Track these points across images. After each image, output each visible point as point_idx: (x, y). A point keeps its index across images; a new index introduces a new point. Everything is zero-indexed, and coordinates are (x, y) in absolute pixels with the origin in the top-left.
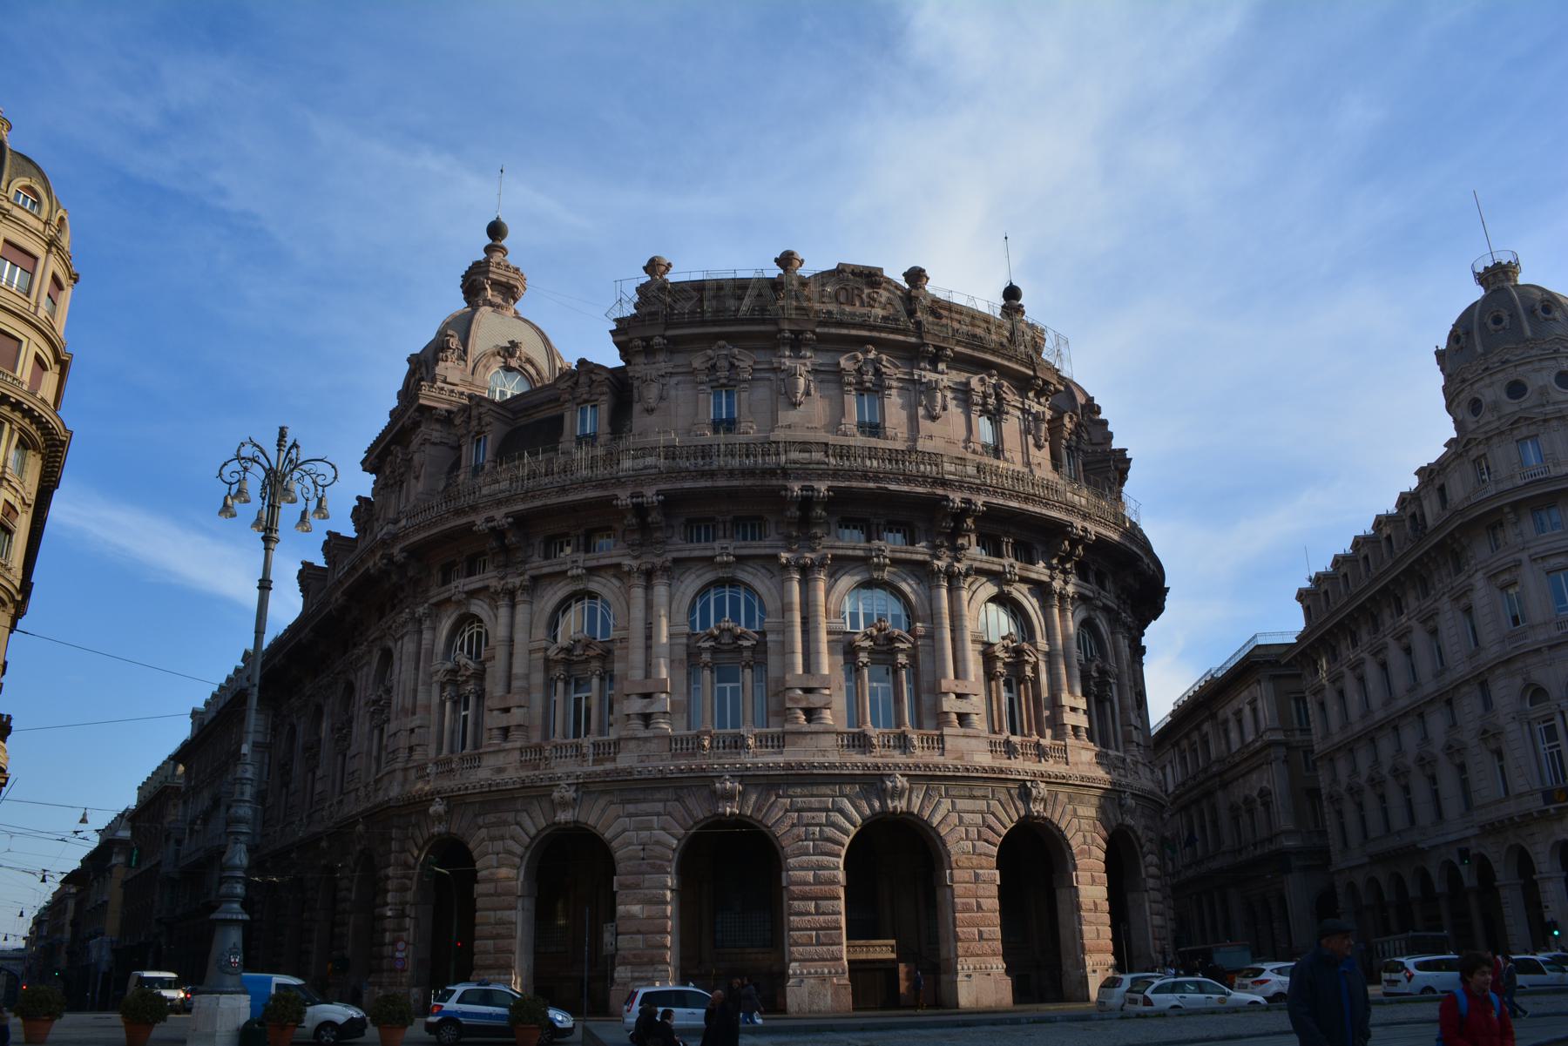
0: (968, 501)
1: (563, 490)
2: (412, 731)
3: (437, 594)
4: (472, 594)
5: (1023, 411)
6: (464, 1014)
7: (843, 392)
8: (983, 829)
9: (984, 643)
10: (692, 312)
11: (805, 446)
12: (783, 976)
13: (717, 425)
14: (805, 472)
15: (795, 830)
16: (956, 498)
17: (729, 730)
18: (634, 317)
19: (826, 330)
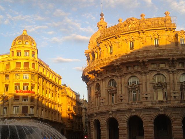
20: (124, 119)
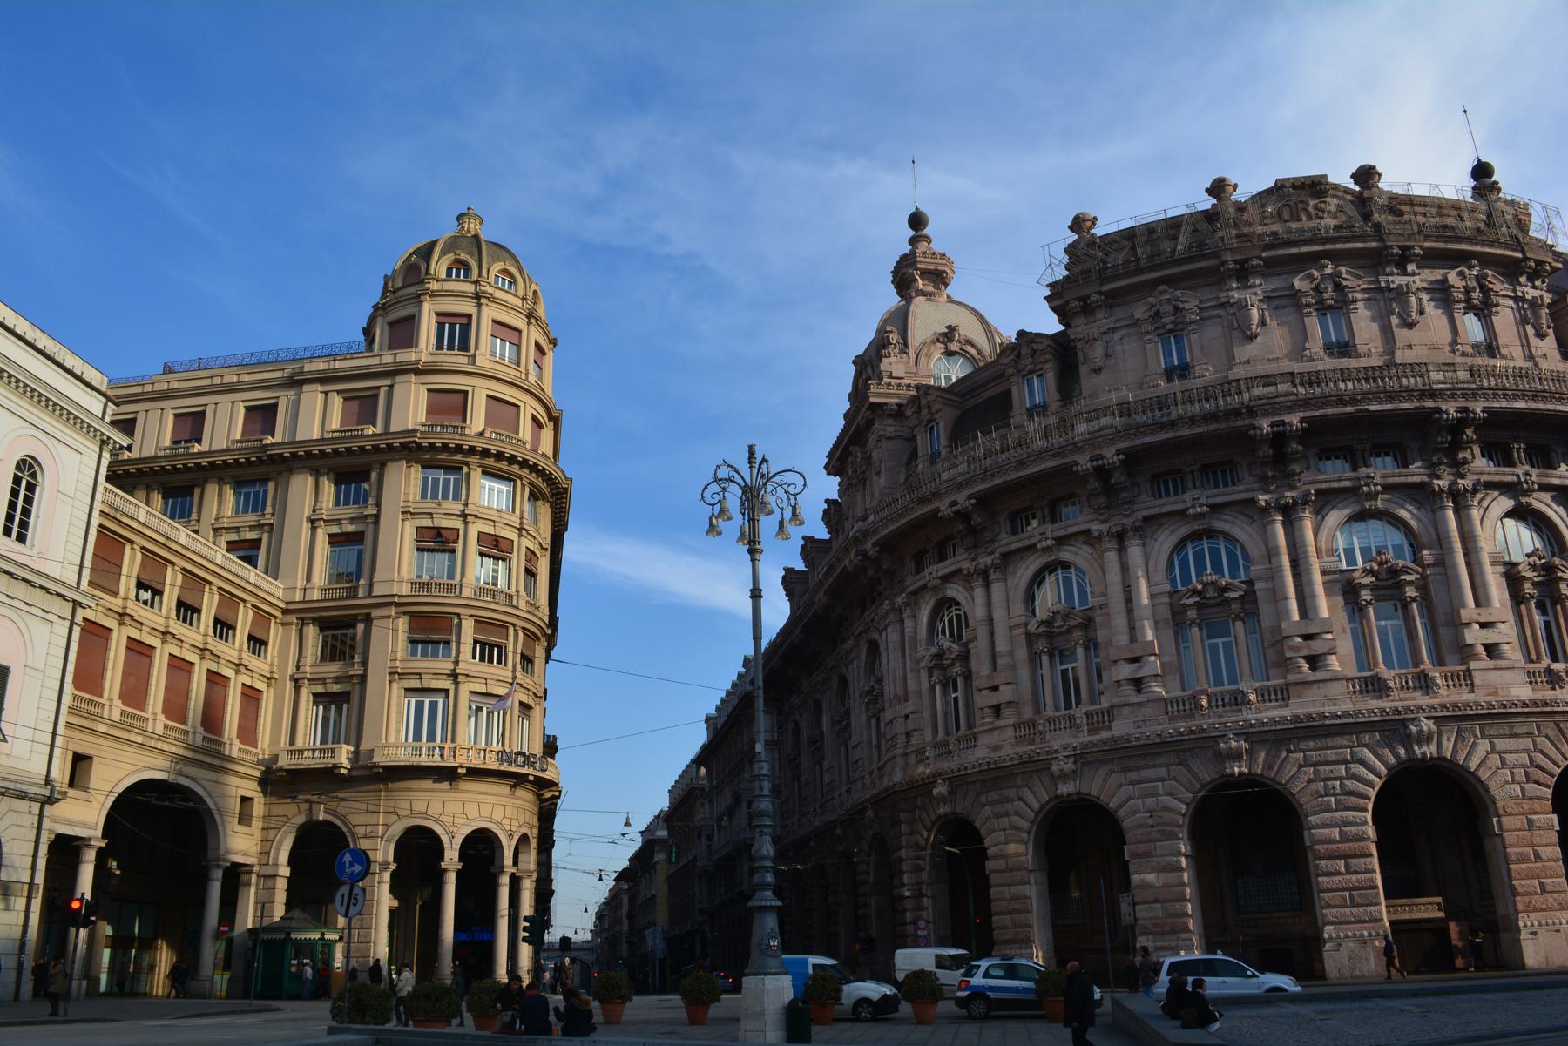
0: (1465, 410)
1: (1021, 464)
2: (907, 717)
3: (912, 583)
4: (947, 578)
5: (1516, 299)
6: (992, 988)
7: (1302, 316)
8: (1531, 770)
9: (1505, 564)
10: (1127, 262)
11: (1269, 379)
12: (1317, 941)
13: (1169, 373)
14: (1273, 406)
15: (1313, 786)
16: (1450, 408)
17: (1227, 687)
18: (1066, 278)
19: (1273, 253)
20: (1351, 785)
